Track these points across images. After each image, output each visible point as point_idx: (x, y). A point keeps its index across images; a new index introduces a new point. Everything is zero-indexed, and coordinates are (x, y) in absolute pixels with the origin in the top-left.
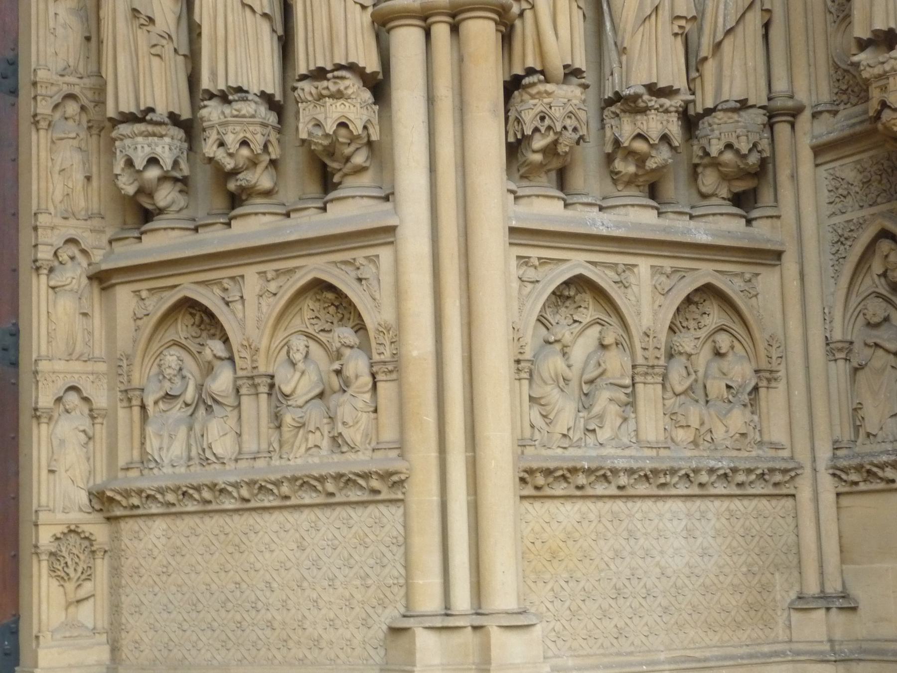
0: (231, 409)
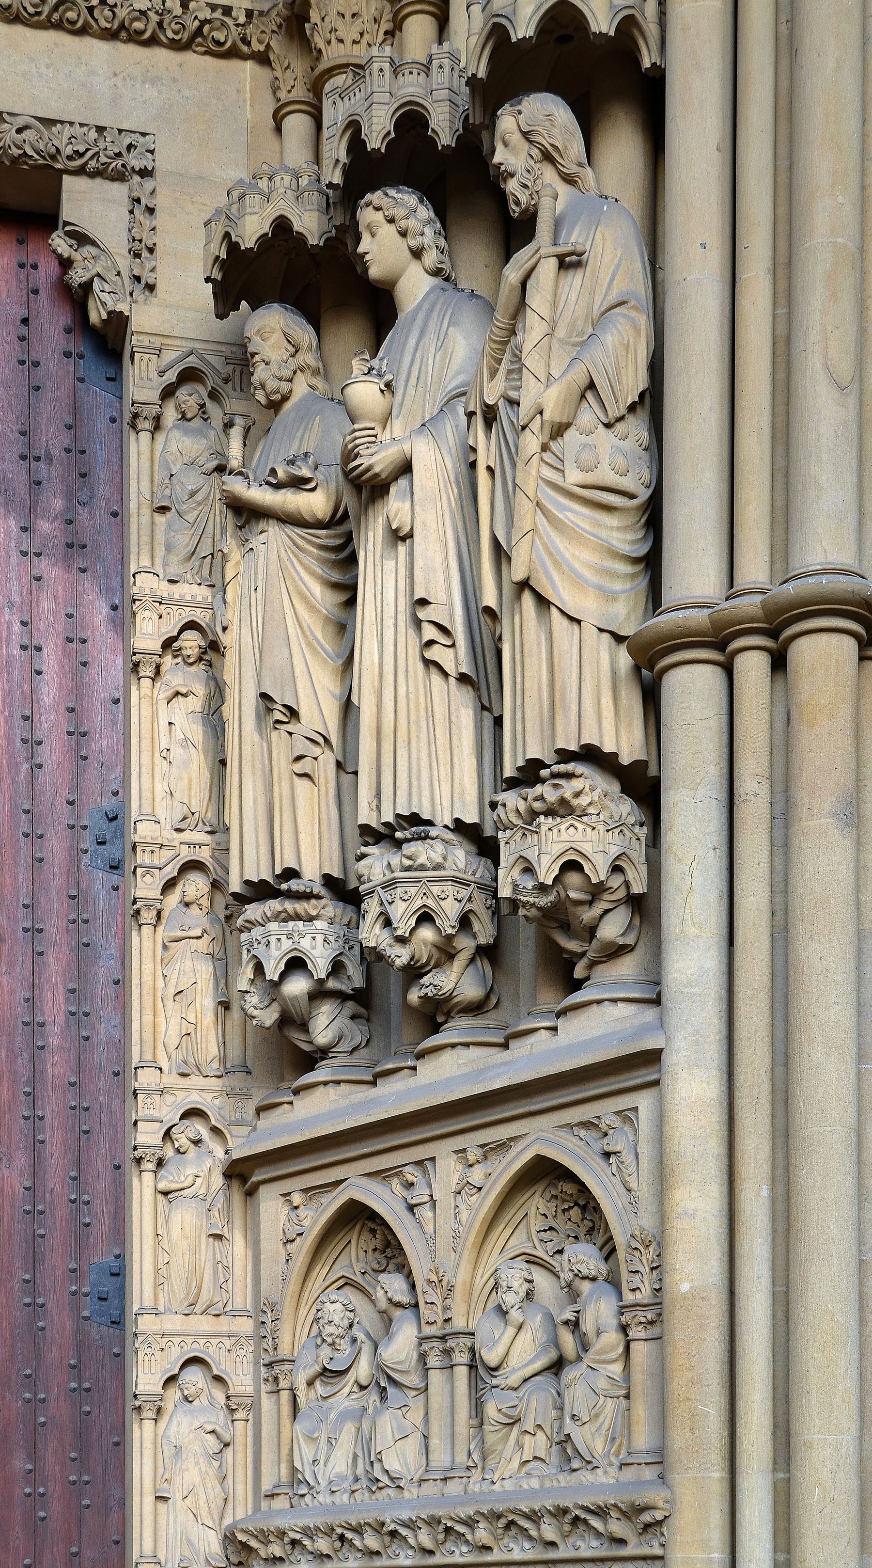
0: (414, 1393)
